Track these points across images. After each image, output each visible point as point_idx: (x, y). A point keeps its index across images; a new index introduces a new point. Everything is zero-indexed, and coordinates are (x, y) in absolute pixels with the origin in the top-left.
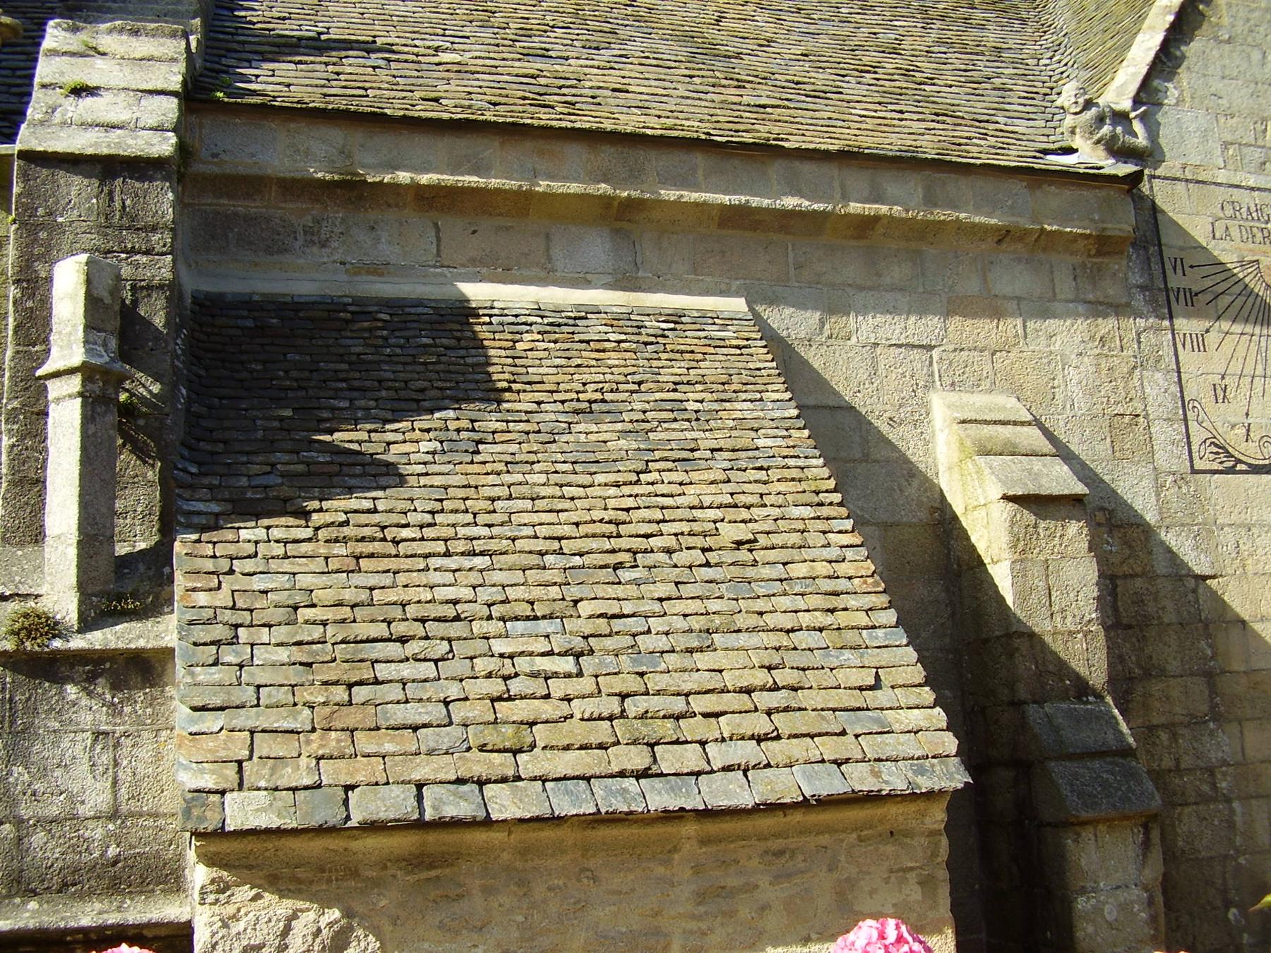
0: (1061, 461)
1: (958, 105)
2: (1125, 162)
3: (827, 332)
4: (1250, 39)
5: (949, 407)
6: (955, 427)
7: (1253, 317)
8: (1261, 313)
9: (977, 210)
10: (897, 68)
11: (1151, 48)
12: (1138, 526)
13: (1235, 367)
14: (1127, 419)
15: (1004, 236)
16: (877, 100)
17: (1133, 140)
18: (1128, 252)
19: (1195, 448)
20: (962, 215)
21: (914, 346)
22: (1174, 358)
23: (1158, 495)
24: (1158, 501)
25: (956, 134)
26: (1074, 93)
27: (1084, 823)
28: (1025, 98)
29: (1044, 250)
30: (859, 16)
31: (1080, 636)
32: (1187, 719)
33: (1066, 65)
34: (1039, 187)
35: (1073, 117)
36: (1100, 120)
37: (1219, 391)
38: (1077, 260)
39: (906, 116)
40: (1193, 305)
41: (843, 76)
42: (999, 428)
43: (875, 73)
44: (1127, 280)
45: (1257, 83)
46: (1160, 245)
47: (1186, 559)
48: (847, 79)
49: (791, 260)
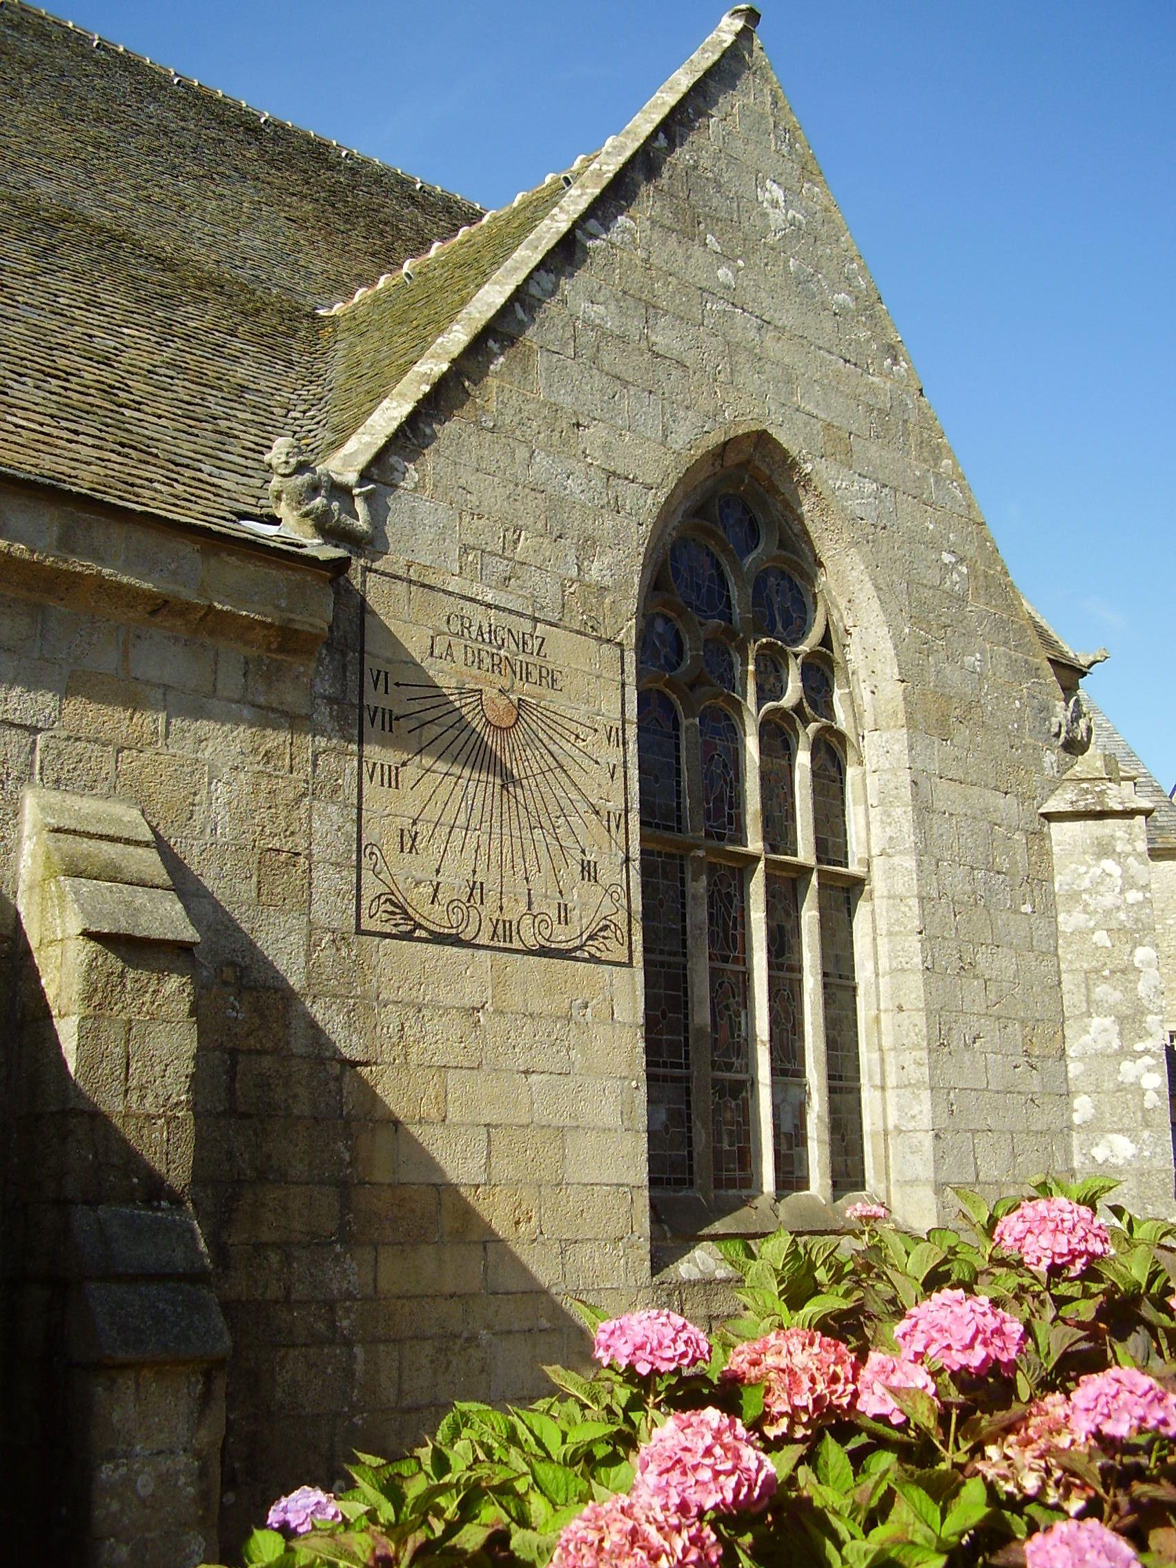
0: (175, 897)
1: (158, 440)
2: (337, 546)
4: (518, 433)
5: (43, 809)
6: (45, 835)
7: (462, 757)
8: (475, 752)
9: (127, 568)
10: (98, 381)
11: (395, 419)
12: (276, 990)
13: (432, 813)
15: (160, 606)
16: (49, 411)
17: (350, 521)
18: (321, 654)
19: (365, 903)
20: (106, 571)
21: (12, 725)
23: (308, 955)
24: (307, 962)
25: (134, 472)
26: (286, 450)
27: (123, 1367)
28: (250, 449)
29: (211, 633)
30: (78, 312)
31: (161, 1122)
32: (308, 1238)
33: (318, 423)
34: (217, 554)
35: (280, 479)
36: (314, 489)
37: (406, 838)
38: (253, 652)
39: (81, 438)
40: (391, 730)
41: (21, 375)
42: (105, 845)
43: (67, 381)
44: (312, 686)
45: (517, 485)
46: (362, 652)
47: (333, 1037)
48: (23, 379)
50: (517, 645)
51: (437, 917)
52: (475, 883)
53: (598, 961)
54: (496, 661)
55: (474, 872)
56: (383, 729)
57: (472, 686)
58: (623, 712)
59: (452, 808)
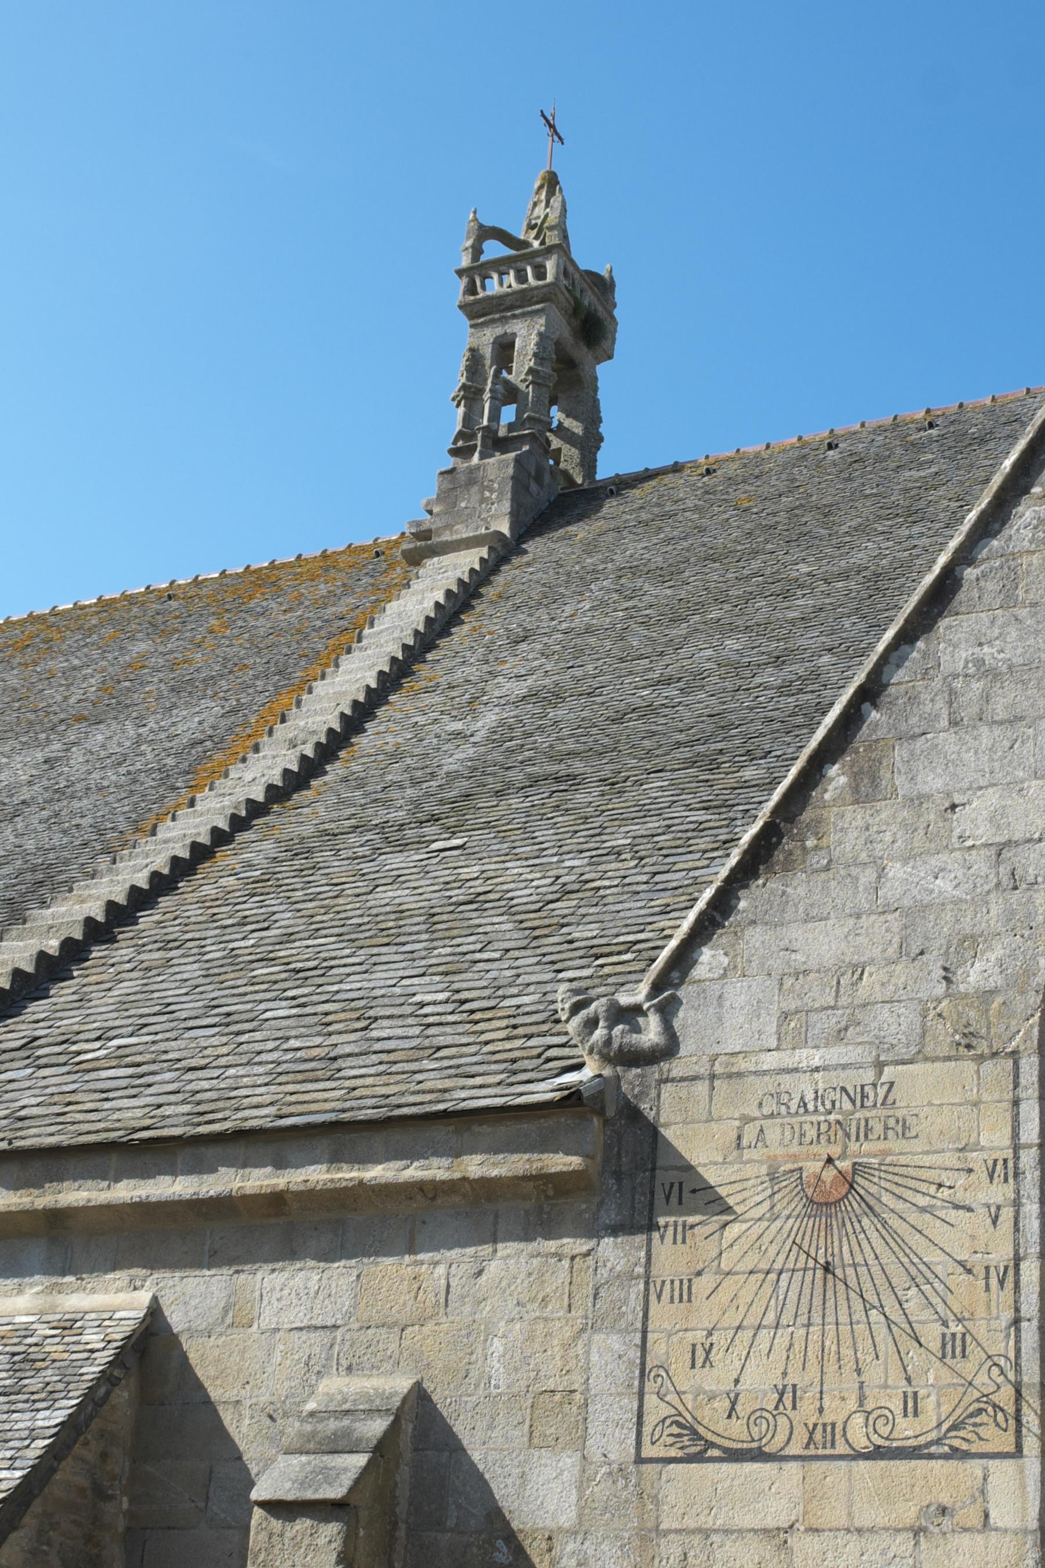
3: (229, 1320)
13: (733, 1319)
14: (558, 1397)
19: (647, 1430)
21: (316, 1328)
22: (641, 1314)
24: (580, 1499)
40: (684, 1242)
46: (653, 1169)
49: (206, 1247)
50: (853, 1102)
51: (736, 1434)
52: (785, 1386)
53: (966, 1455)
54: (824, 1127)
55: (785, 1374)
56: (675, 1242)
57: (789, 1166)
58: (1015, 1134)
59: (757, 1309)
